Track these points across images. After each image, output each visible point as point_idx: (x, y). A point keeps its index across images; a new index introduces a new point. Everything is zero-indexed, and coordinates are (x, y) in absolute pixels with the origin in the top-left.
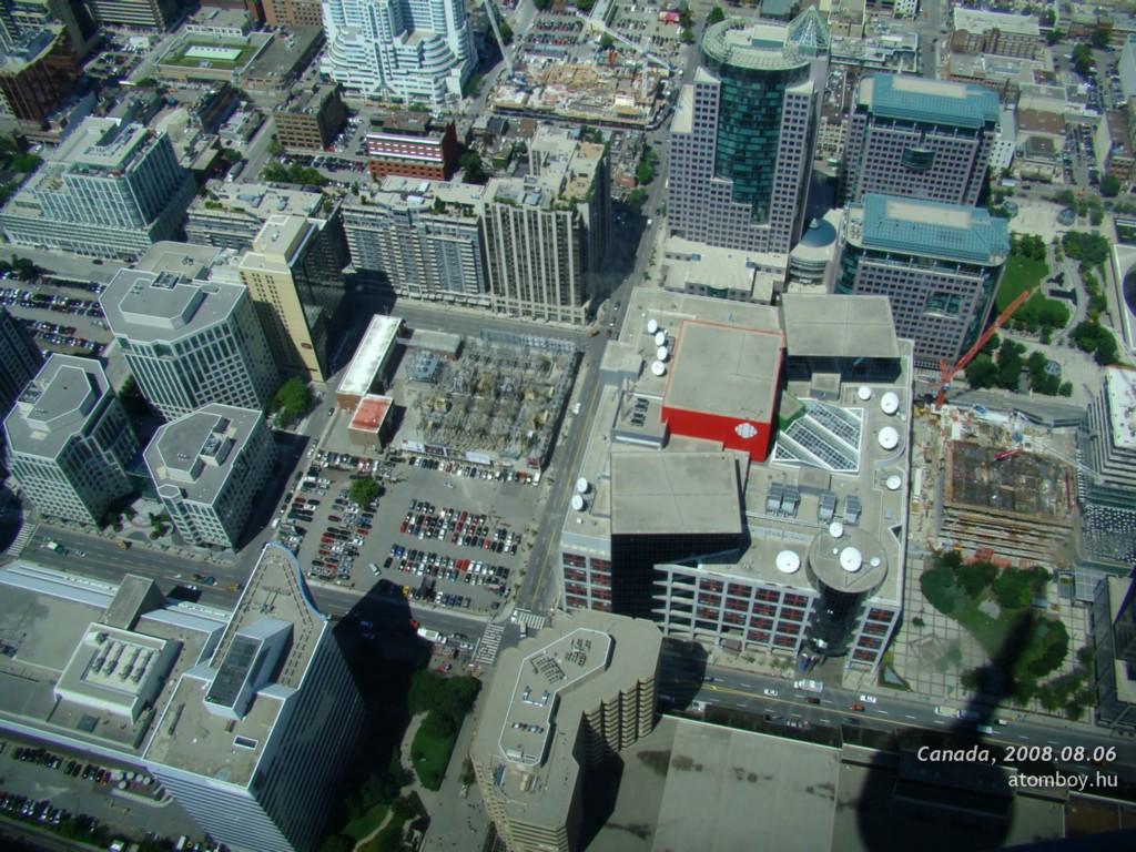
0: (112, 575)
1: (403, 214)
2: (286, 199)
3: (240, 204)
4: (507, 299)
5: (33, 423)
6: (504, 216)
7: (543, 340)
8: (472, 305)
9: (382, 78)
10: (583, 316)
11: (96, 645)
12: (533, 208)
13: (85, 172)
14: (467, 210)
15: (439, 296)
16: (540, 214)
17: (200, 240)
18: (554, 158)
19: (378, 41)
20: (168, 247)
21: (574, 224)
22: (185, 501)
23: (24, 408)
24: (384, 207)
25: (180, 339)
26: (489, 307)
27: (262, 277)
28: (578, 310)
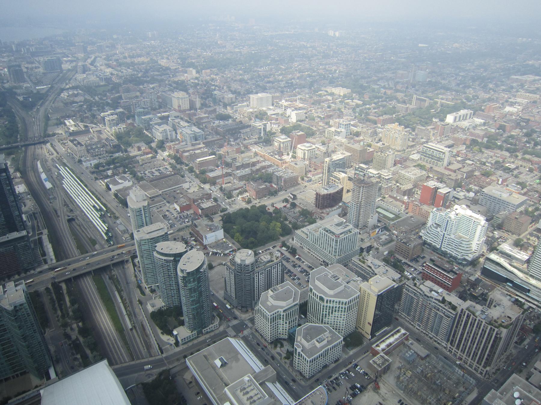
0: (265, 362)
1: (428, 297)
2: (387, 270)
3: (371, 265)
4: (454, 349)
5: (270, 299)
6: (468, 317)
7: (462, 373)
8: (438, 343)
9: (441, 246)
10: (484, 373)
11: (246, 382)
12: (481, 320)
13: (327, 231)
14: (454, 308)
15: (427, 333)
16: (484, 323)
17: (352, 270)
18: (499, 305)
19: (446, 233)
20: (340, 267)
21: (497, 334)
22: (301, 353)
23: (270, 292)
24: (422, 291)
25: (329, 299)
26: (445, 348)
27: (367, 293)
28: (483, 369)
